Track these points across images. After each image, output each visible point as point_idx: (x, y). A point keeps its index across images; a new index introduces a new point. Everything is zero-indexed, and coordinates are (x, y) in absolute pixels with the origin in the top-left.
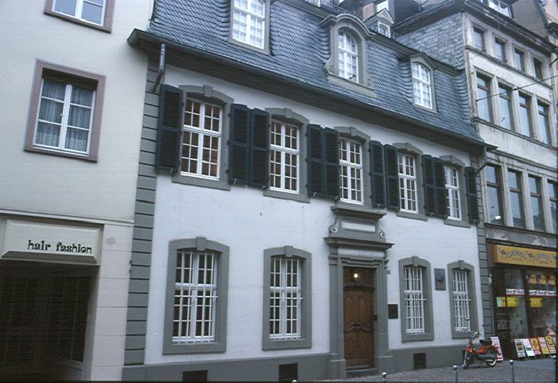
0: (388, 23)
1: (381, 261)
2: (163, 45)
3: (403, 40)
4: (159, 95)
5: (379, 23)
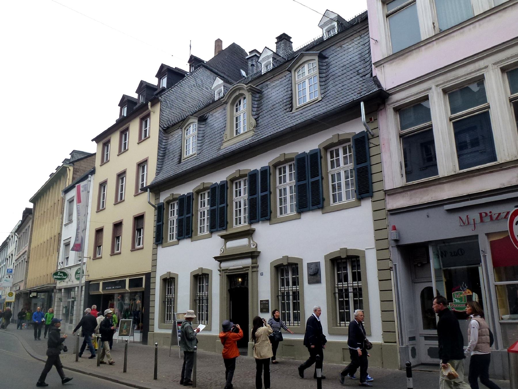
1: (249, 267)
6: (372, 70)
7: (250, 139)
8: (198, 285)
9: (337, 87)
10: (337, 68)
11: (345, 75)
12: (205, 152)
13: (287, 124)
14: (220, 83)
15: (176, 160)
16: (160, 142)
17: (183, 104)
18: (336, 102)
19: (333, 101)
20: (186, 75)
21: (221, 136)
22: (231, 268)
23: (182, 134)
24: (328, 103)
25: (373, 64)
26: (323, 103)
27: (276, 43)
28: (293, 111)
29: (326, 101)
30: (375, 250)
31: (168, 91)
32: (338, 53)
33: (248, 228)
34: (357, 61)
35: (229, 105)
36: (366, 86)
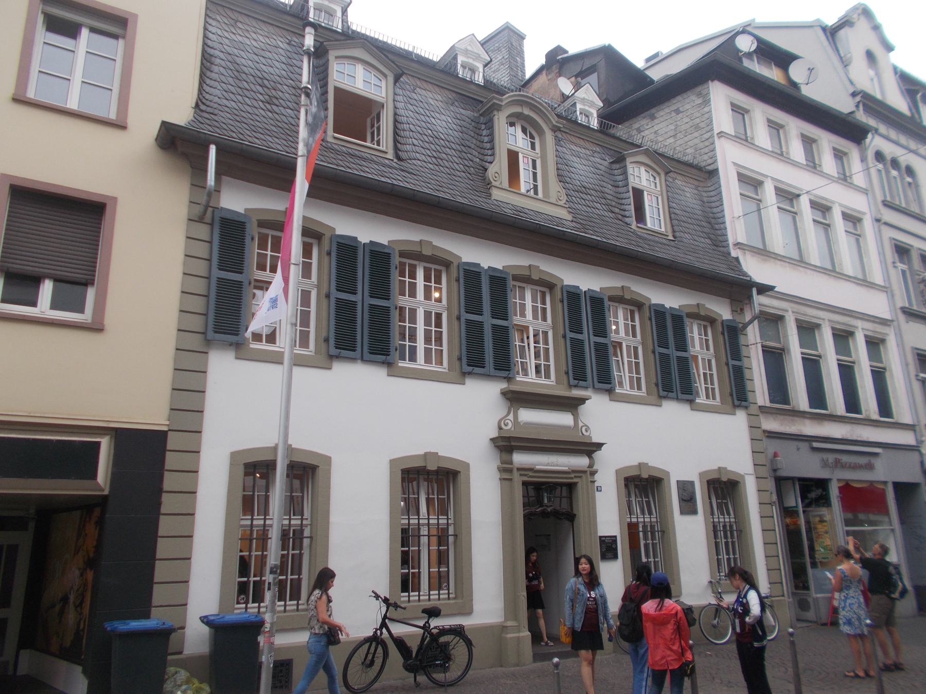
0: (592, 104)
1: (584, 472)
2: (213, 149)
3: (621, 131)
4: (212, 224)
5: (579, 106)
22: (537, 467)
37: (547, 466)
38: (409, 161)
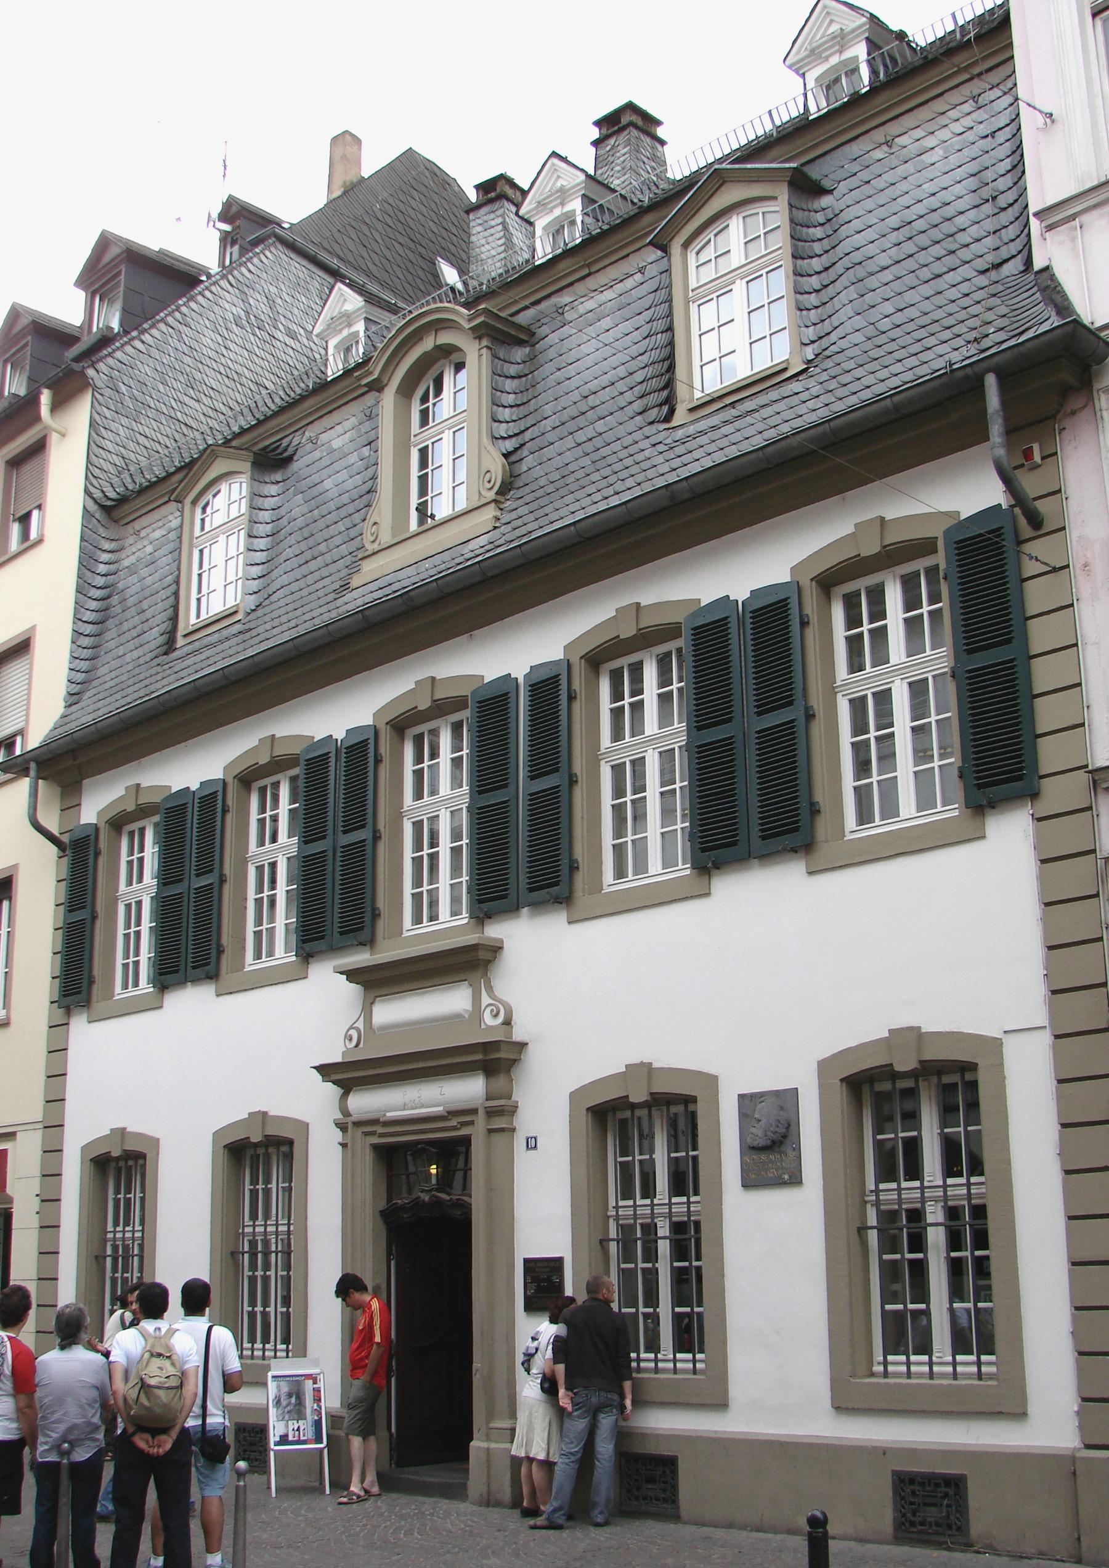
1: (474, 1111)
6: (1028, 243)
7: (483, 540)
8: (248, 1187)
9: (874, 315)
10: (870, 234)
11: (910, 264)
12: (282, 603)
13: (651, 474)
14: (349, 307)
15: (155, 637)
16: (87, 561)
17: (187, 400)
18: (869, 380)
19: (859, 373)
20: (204, 278)
21: (353, 533)
22: (388, 1114)
23: (181, 526)
24: (833, 384)
25: (1036, 215)
26: (811, 383)
27: (596, 143)
28: (677, 420)
29: (825, 376)
30: (1045, 1039)
31: (126, 343)
32: (876, 169)
33: (471, 939)
34: (961, 205)
35: (388, 398)
36: (1003, 310)
37: (404, 1110)
38: (267, 602)
